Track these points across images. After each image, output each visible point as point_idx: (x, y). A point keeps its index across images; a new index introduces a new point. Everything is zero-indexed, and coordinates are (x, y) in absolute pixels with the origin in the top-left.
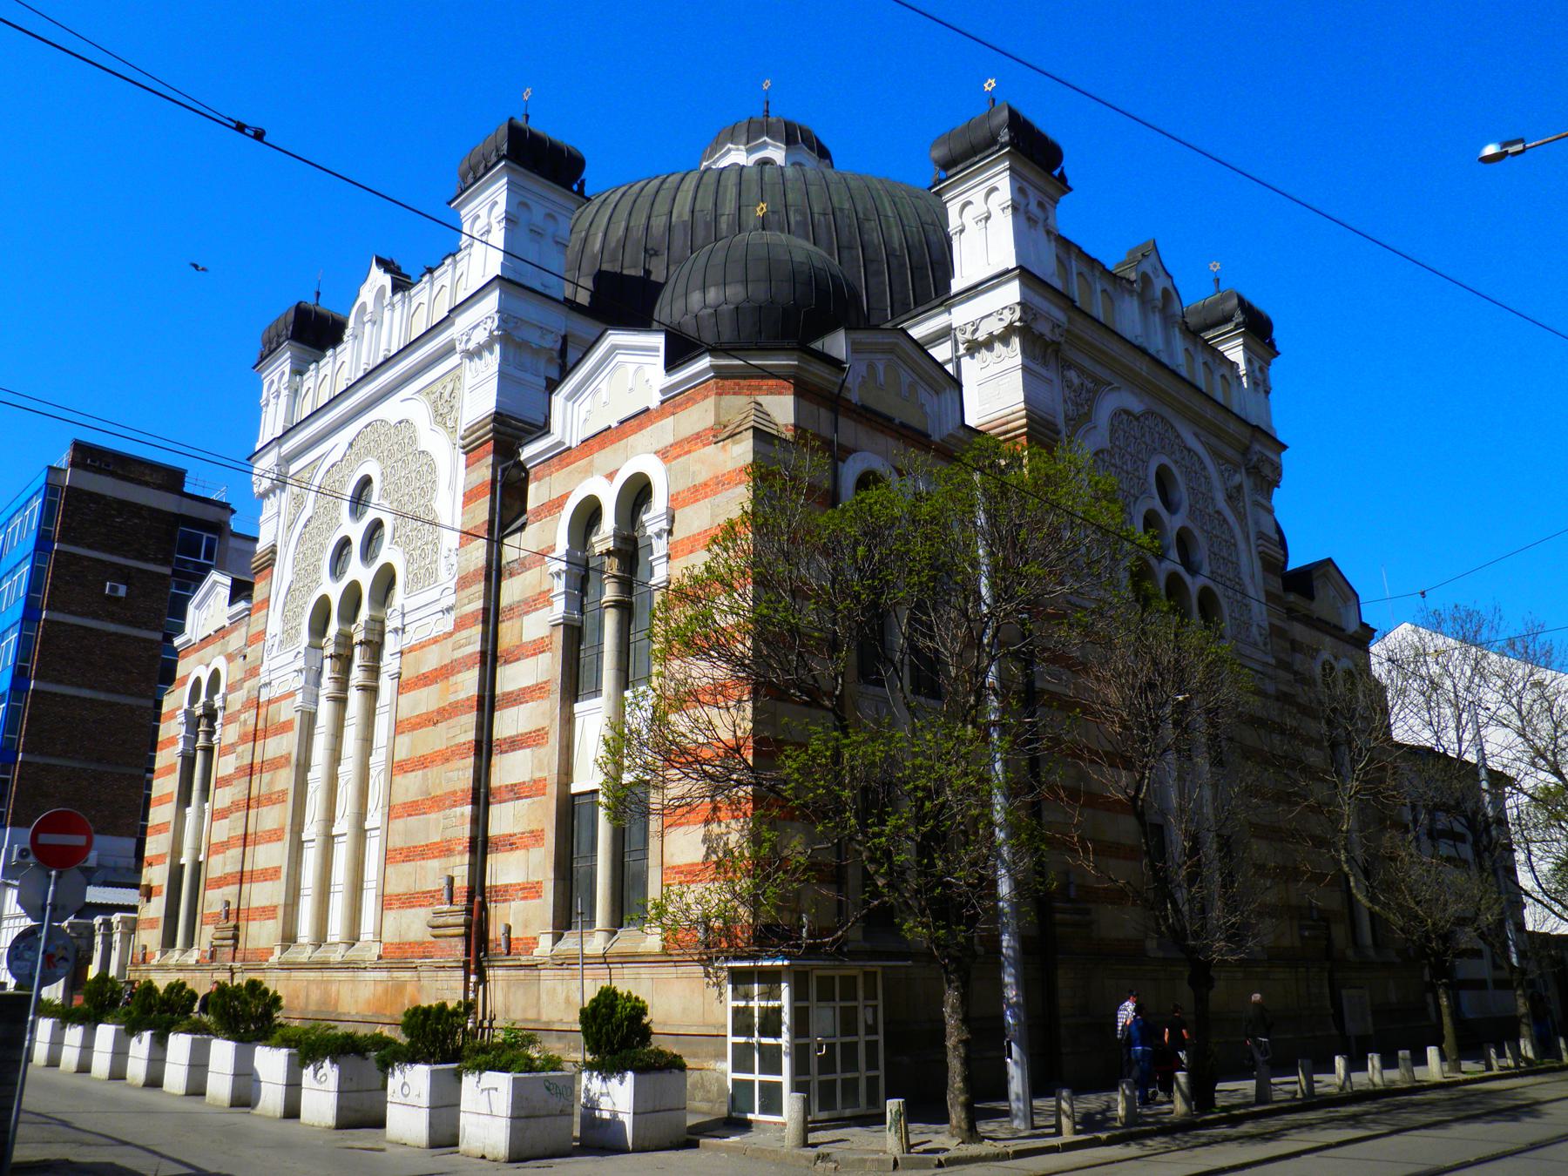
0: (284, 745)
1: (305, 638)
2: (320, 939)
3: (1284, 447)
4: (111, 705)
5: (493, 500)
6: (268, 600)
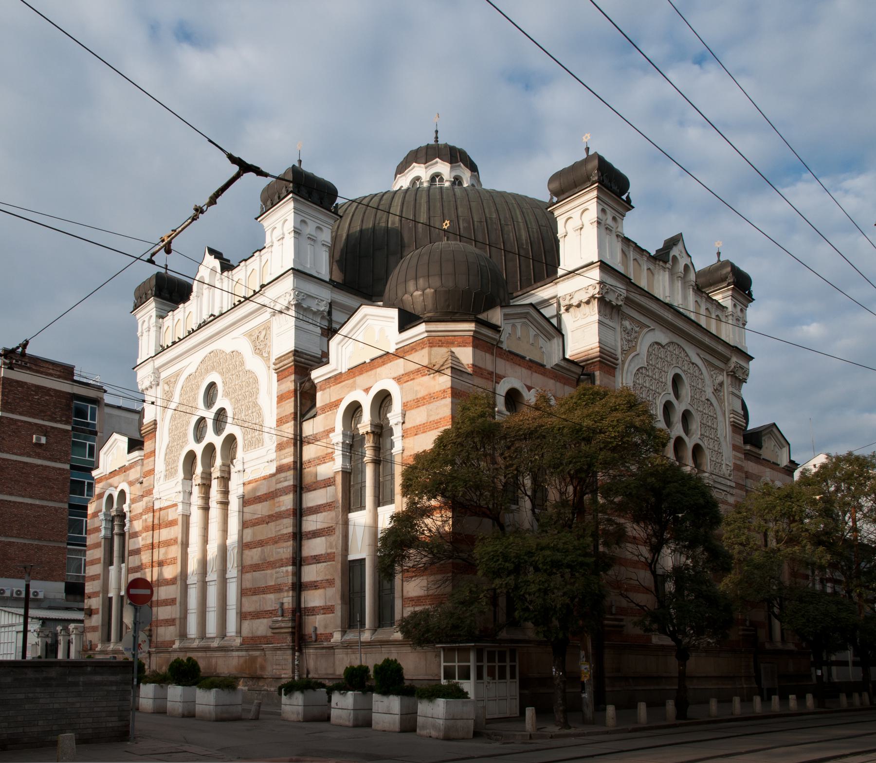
3: (751, 358)
4: (43, 507)
5: (296, 401)
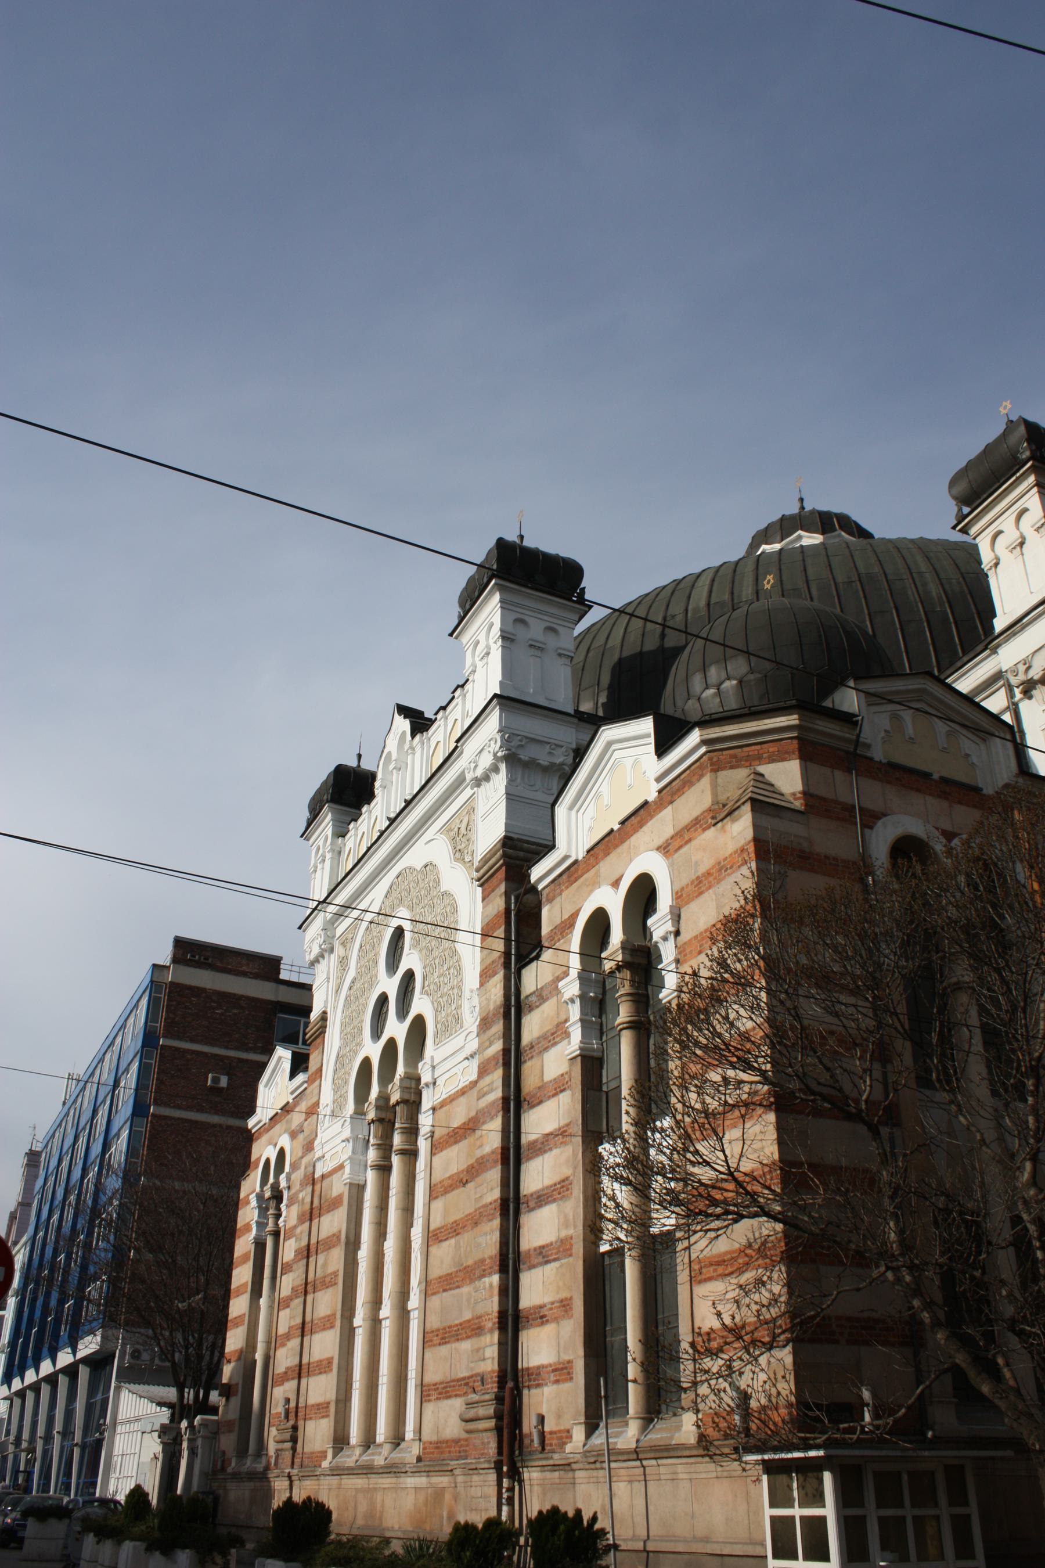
0: (333, 1223)
1: (350, 1107)
2: (369, 1441)
6: (320, 1069)
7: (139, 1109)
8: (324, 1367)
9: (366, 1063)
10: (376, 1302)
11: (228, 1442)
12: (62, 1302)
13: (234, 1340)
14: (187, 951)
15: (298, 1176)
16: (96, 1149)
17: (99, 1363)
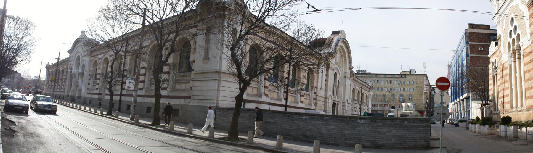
0: (507, 71)
1: (507, 51)
7: (467, 55)
8: (508, 95)
9: (509, 43)
10: (516, 84)
11: (492, 109)
12: (459, 89)
13: (491, 93)
14: (471, 26)
15: (499, 64)
16: (460, 63)
17: (467, 98)
